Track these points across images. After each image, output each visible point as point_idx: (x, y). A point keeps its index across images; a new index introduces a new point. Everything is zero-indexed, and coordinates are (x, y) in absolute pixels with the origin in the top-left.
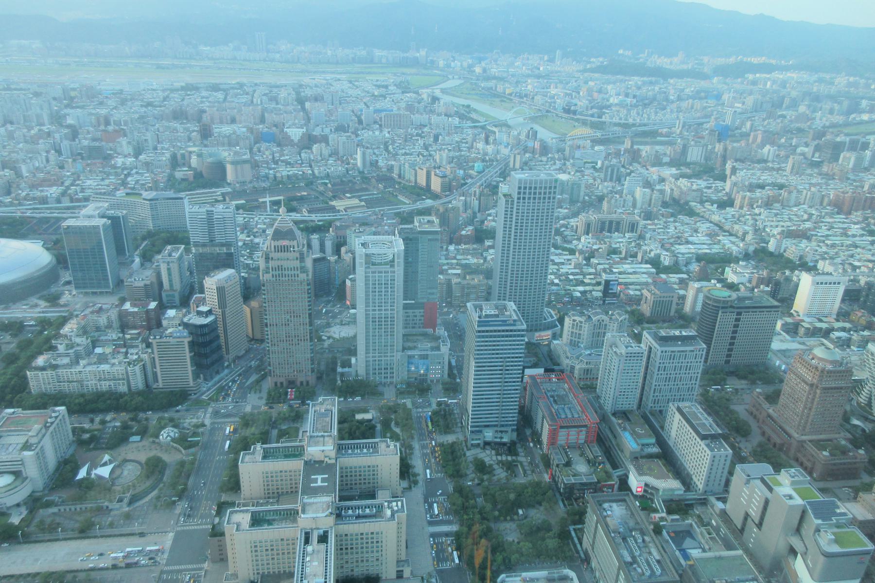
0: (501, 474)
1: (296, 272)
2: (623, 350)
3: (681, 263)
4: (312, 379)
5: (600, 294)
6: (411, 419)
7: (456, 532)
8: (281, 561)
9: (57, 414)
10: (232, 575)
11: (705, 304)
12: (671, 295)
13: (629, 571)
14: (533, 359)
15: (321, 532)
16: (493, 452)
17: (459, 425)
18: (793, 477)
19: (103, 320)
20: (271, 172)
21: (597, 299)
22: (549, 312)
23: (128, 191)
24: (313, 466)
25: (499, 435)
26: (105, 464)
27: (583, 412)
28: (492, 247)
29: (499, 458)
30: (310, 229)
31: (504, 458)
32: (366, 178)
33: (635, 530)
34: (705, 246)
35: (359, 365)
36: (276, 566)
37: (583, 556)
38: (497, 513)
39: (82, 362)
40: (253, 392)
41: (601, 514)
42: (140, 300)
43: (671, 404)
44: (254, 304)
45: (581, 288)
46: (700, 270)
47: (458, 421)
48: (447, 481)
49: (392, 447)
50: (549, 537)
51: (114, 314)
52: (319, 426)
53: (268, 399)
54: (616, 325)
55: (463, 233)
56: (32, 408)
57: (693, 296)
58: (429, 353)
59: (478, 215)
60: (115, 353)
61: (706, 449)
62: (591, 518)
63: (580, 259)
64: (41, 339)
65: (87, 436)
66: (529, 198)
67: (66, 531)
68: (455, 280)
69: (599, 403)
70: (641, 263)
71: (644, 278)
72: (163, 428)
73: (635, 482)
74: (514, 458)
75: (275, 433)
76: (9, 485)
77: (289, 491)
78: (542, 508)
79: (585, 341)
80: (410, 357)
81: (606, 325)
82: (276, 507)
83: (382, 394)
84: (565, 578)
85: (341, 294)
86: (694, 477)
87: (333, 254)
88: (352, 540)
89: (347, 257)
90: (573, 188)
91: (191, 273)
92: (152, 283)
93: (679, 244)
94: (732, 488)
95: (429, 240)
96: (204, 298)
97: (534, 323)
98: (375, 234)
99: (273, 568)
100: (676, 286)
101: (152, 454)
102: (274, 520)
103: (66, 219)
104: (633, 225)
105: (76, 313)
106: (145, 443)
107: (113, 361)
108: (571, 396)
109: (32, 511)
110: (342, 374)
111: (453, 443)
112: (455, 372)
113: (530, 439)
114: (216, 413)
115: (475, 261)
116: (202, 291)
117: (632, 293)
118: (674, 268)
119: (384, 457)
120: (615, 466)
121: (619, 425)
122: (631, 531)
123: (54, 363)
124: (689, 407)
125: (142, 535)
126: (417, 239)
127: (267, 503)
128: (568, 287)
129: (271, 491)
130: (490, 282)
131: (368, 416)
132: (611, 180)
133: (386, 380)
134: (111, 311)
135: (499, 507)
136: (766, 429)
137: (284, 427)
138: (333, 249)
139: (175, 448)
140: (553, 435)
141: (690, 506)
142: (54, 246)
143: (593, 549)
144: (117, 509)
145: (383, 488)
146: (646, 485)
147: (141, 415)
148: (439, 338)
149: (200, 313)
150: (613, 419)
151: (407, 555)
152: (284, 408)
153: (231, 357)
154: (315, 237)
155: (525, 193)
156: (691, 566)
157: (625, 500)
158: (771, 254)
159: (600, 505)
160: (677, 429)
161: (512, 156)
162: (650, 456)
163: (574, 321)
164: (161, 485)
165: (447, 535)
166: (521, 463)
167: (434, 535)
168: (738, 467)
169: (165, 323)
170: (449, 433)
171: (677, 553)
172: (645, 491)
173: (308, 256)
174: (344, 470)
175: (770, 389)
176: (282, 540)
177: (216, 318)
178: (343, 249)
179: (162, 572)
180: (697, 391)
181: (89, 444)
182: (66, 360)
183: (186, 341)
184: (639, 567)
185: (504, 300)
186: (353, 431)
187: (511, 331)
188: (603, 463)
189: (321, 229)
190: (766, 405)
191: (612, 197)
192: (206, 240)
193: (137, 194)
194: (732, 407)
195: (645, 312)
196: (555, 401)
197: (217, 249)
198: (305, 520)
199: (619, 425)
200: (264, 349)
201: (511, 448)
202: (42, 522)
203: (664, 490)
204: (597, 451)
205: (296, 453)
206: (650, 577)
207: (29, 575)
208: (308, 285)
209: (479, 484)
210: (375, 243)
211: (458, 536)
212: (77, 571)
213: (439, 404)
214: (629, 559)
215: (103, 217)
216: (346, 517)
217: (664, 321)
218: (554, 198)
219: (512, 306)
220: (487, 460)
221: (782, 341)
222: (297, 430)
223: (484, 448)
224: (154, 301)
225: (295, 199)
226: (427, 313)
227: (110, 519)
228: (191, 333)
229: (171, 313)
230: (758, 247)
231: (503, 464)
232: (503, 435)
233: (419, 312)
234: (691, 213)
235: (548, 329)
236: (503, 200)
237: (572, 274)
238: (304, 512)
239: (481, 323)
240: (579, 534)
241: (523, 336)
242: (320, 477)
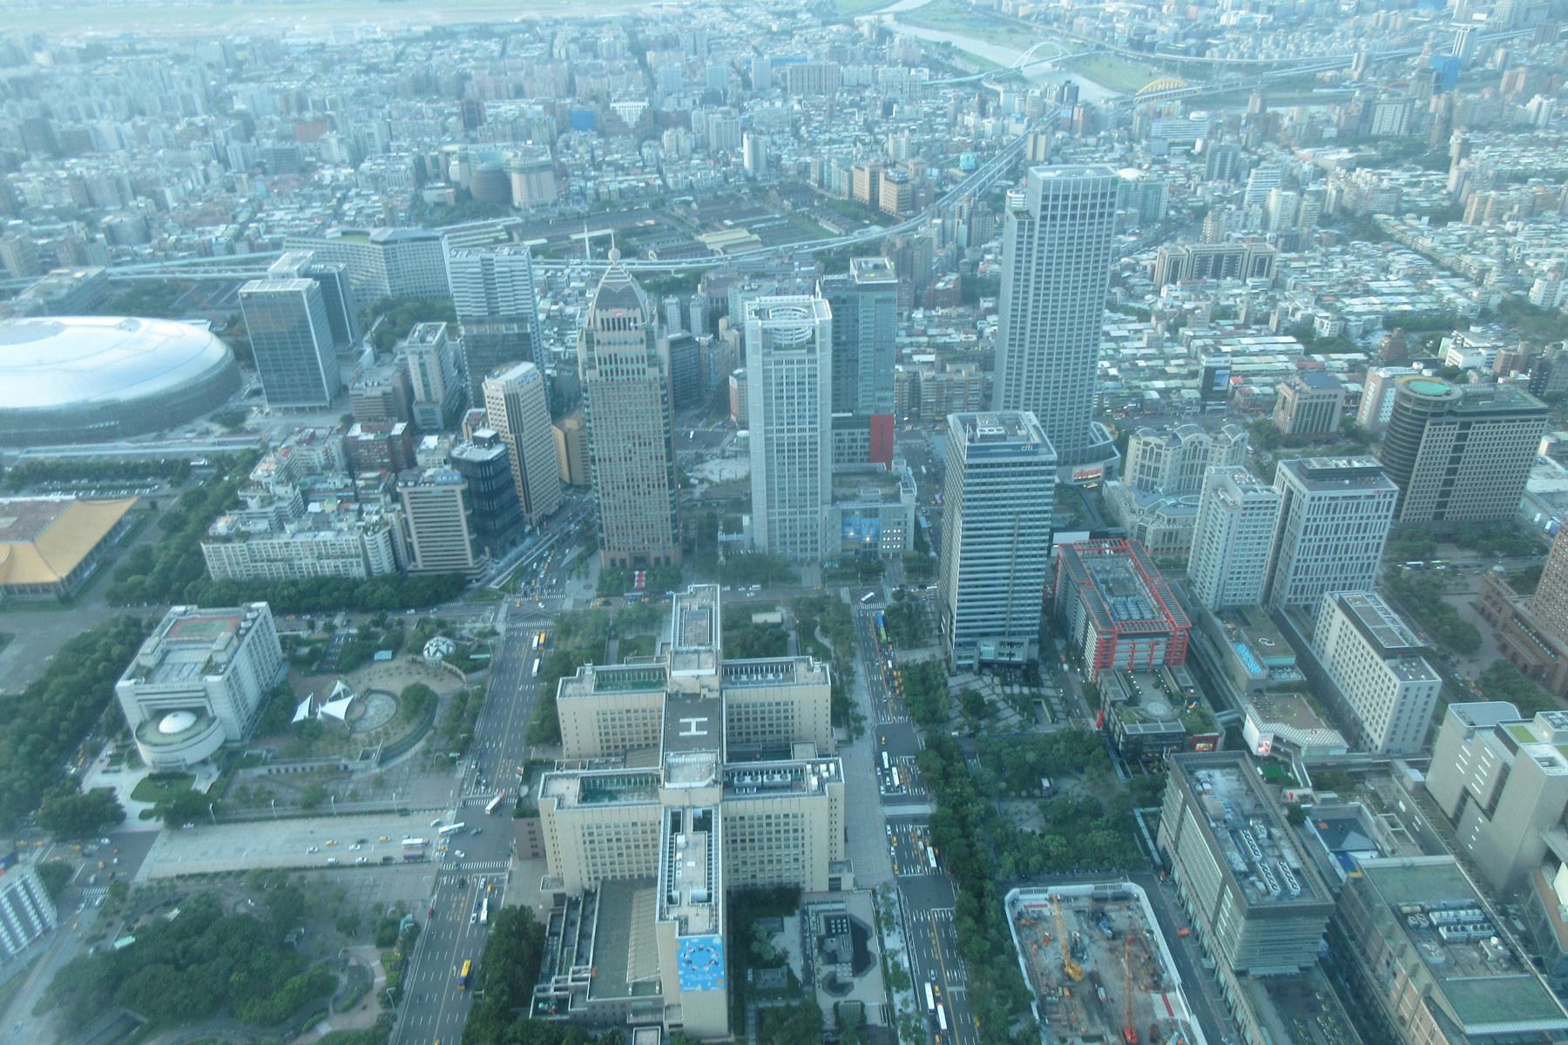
0: (1011, 718)
1: (640, 366)
2: (1238, 497)
3: (1354, 331)
4: (674, 553)
5: (1196, 394)
6: (849, 622)
7: (932, 817)
8: (634, 859)
9: (255, 614)
10: (553, 880)
11: (1398, 410)
12: (1333, 392)
13: (1242, 888)
14: (1069, 515)
15: (699, 812)
16: (997, 680)
17: (936, 632)
18: (1558, 726)
19: (317, 456)
20: (590, 184)
21: (1189, 402)
22: (1100, 430)
23: (346, 228)
24: (682, 703)
25: (1007, 650)
26: (337, 697)
27: (1161, 609)
28: (993, 311)
29: (1008, 690)
30: (663, 287)
31: (1016, 689)
32: (761, 190)
33: (1254, 816)
34: (1403, 299)
35: (756, 527)
36: (626, 867)
37: (1157, 859)
38: (1003, 785)
39: (289, 528)
40: (574, 577)
41: (1193, 789)
42: (376, 420)
43: (1326, 595)
44: (571, 423)
45: (1160, 384)
46: (1392, 345)
47: (933, 625)
48: (914, 730)
49: (817, 671)
50: (1096, 828)
51: (335, 445)
52: (690, 635)
53: (600, 589)
54: (1225, 451)
55: (940, 285)
56: (214, 604)
57: (1375, 394)
58: (880, 505)
59: (967, 252)
60: (341, 511)
61: (1391, 674)
62: (1174, 795)
63: (1159, 329)
64: (219, 489)
65: (305, 650)
66: (1064, 217)
67: (283, 804)
68: (925, 374)
69: (1191, 592)
70: (1276, 334)
71: (1281, 362)
72: (430, 637)
73: (1257, 736)
74: (1034, 690)
75: (614, 646)
76: (187, 730)
77: (643, 743)
78: (1084, 778)
79: (1166, 480)
80: (845, 513)
81: (1206, 451)
82: (621, 770)
83: (797, 579)
84: (1124, 898)
85: (721, 403)
86: (1366, 725)
88: (751, 826)
89: (730, 336)
90: (1146, 196)
91: (460, 372)
92: (394, 389)
93: (1352, 296)
94: (1440, 745)
95: (877, 301)
96: (485, 415)
97: (1071, 449)
98: (778, 292)
99: (622, 870)
100: (1342, 377)
101: (412, 681)
102: (619, 792)
104: (1262, 262)
105: (272, 444)
106: (402, 661)
107: (339, 525)
108: (1139, 581)
109: (227, 773)
110: (727, 545)
111: (927, 663)
112: (927, 539)
113: (1063, 658)
114: (514, 615)
115: (962, 337)
116: (480, 402)
117: (1256, 390)
118: (1341, 342)
119: (805, 690)
120: (1219, 705)
121: (1229, 632)
122: (1247, 818)
123: (243, 529)
124: (1362, 600)
125: (404, 812)
126: (854, 300)
127: (606, 764)
128: (1135, 383)
129: (612, 744)
130: (989, 377)
131: (774, 618)
132: (1221, 176)
133: (803, 555)
134: (330, 441)
135: (1007, 774)
136: (1508, 637)
137: (629, 637)
139: (450, 671)
140: (1106, 651)
141: (1360, 777)
142: (228, 329)
143: (1176, 848)
144: (363, 771)
145: (803, 741)
146: (1277, 739)
147: (393, 617)
148: (898, 478)
149: (478, 441)
150: (1218, 621)
151: (847, 852)
152: (626, 604)
153: (535, 516)
154: (671, 301)
155: (1054, 207)
156: (1356, 881)
157: (1236, 766)
158: (1535, 310)
159: (1191, 773)
160: (1337, 638)
161: (1031, 138)
162: (1286, 688)
163: (1146, 444)
164: (431, 732)
165: (916, 820)
166: (1047, 700)
167: (891, 821)
168: (1452, 708)
169: (420, 459)
170: (917, 647)
171: (1332, 858)
172: (1274, 749)
173: (660, 336)
174: (735, 710)
175: (1520, 566)
176: (634, 824)
177: (507, 450)
178: (722, 323)
179: (440, 873)
180: (1378, 570)
181: (309, 664)
182: (263, 525)
183: (458, 489)
184: (1261, 880)
185: (1016, 408)
186: (749, 645)
187: (1029, 464)
188: (1197, 699)
189: (683, 286)
190: (1511, 596)
191: (1222, 210)
192: (483, 312)
193: (359, 233)
194: (1446, 599)
195: (1281, 427)
196: (1109, 590)
197: (503, 328)
198: (673, 792)
199: (1229, 632)
200: (591, 501)
201: (1029, 673)
202: (244, 789)
203: (1310, 748)
204: (1186, 677)
205: (654, 680)
206: (1280, 898)
207: (229, 873)
208: (663, 388)
209: (970, 736)
210: (779, 309)
211: (933, 822)
212: (305, 869)
213: (898, 596)
214: (1243, 867)
215: (306, 275)
216: (740, 789)
217: (1317, 442)
218: (1111, 215)
219: (1030, 418)
220: (985, 693)
221: (1549, 476)
222: (652, 642)
223: (980, 673)
224: (400, 421)
225: (633, 232)
226: (874, 431)
227: (351, 786)
228: (465, 476)
229: (431, 441)
230: (1509, 298)
231: (1014, 701)
232: (1014, 650)
233: (861, 433)
234: (1376, 234)
235: (1098, 459)
236: (1013, 217)
237: (1145, 357)
238: (668, 778)
239: (973, 452)
240: (1152, 823)
241: (1050, 473)
242: (693, 721)
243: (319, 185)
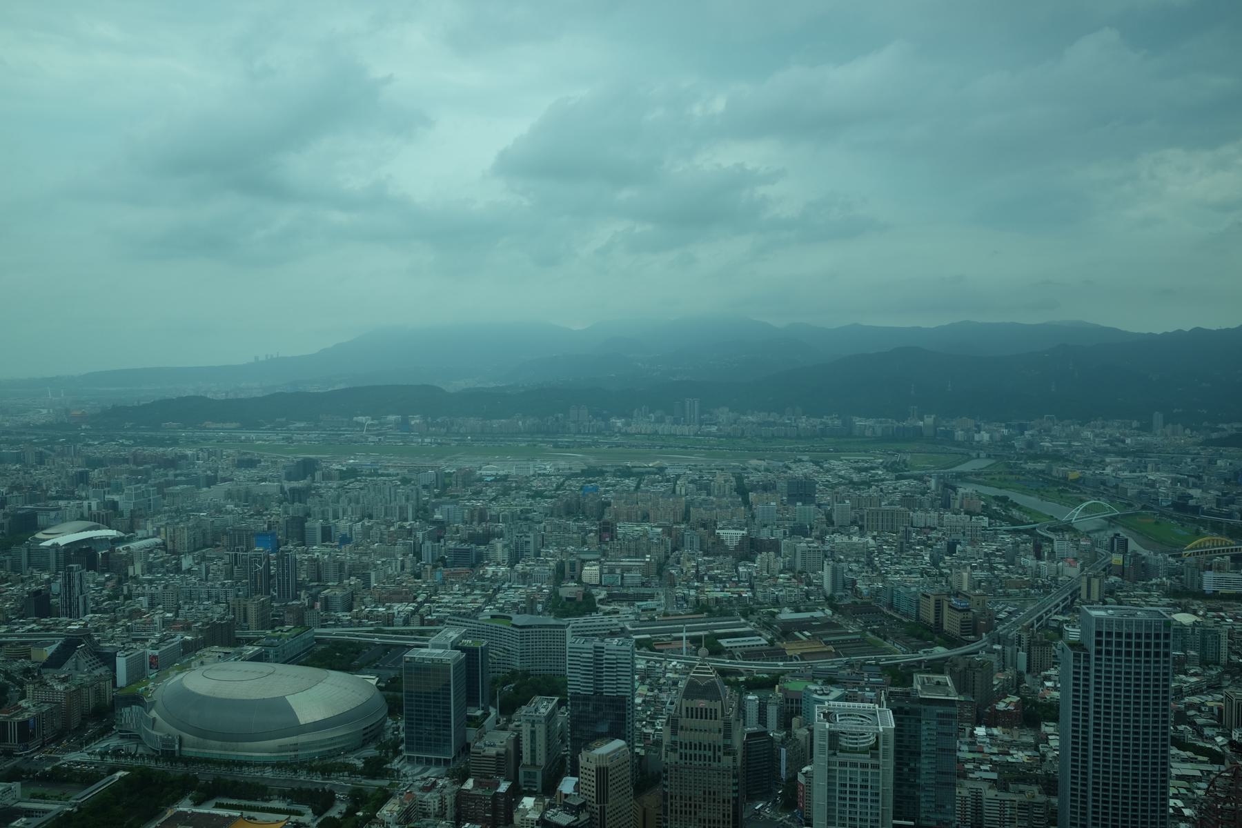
20: (693, 592)
23: (495, 612)
55: (1001, 706)
59: (1028, 678)
87: (779, 728)
89: (801, 733)
103: (410, 647)
130: (1054, 800)
138: (779, 721)
161: (1085, 579)
169: (517, 818)
193: (504, 617)
210: (848, 715)
215: (456, 648)
218: (1167, 655)
229: (528, 802)
243: (481, 578)
